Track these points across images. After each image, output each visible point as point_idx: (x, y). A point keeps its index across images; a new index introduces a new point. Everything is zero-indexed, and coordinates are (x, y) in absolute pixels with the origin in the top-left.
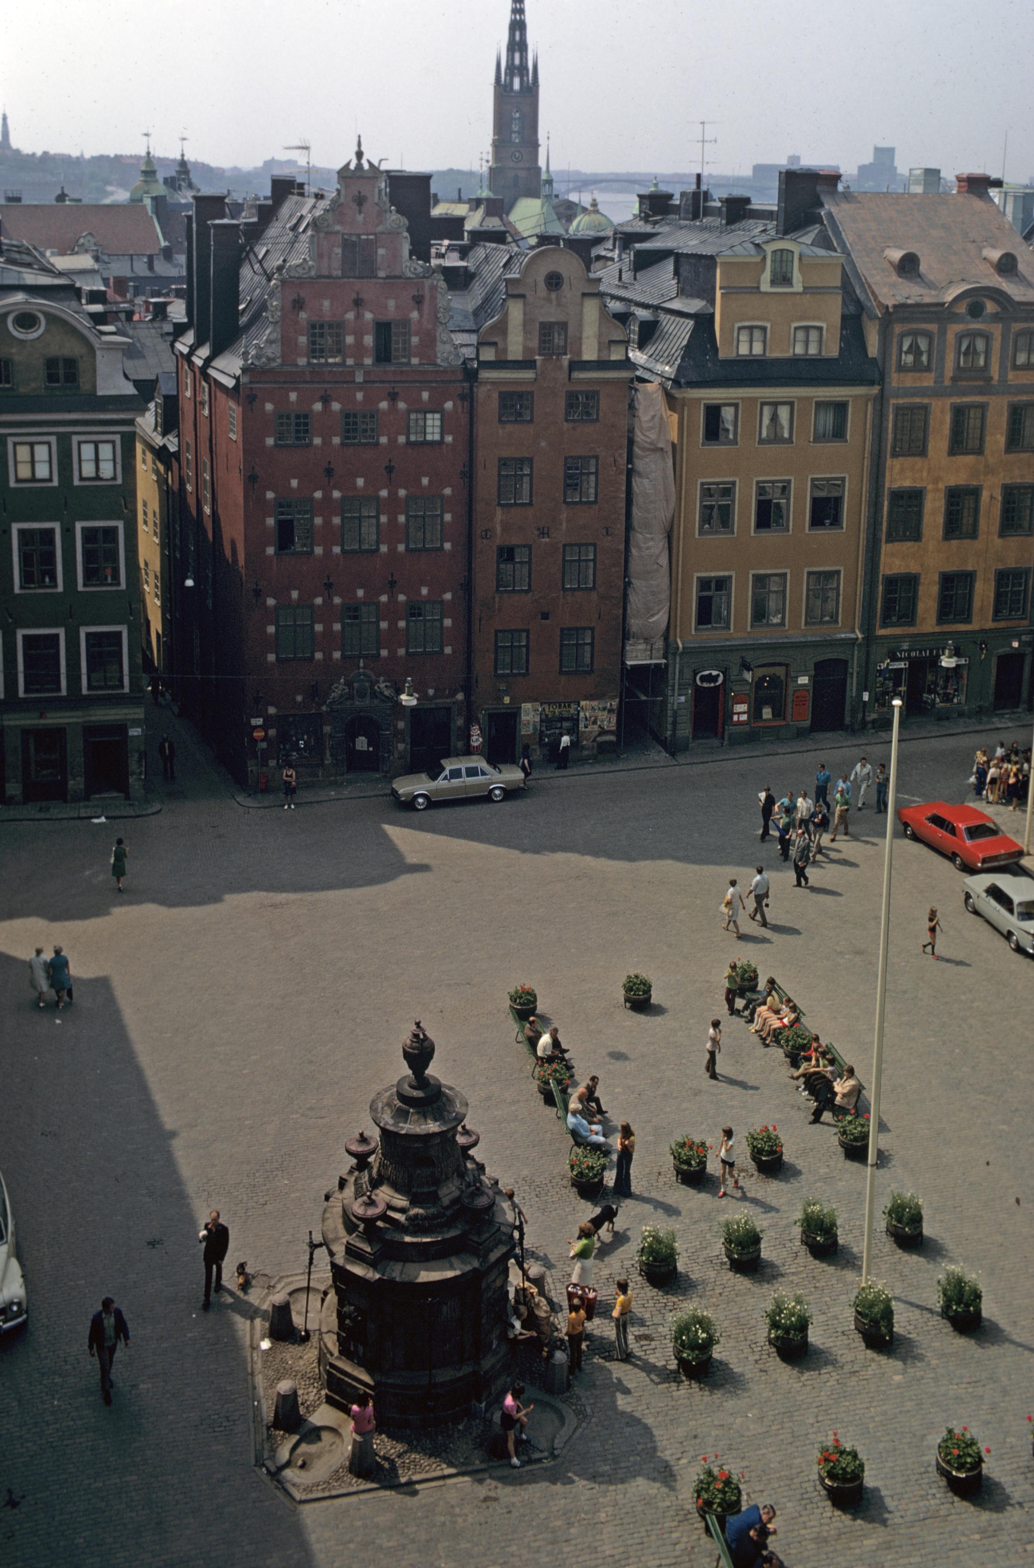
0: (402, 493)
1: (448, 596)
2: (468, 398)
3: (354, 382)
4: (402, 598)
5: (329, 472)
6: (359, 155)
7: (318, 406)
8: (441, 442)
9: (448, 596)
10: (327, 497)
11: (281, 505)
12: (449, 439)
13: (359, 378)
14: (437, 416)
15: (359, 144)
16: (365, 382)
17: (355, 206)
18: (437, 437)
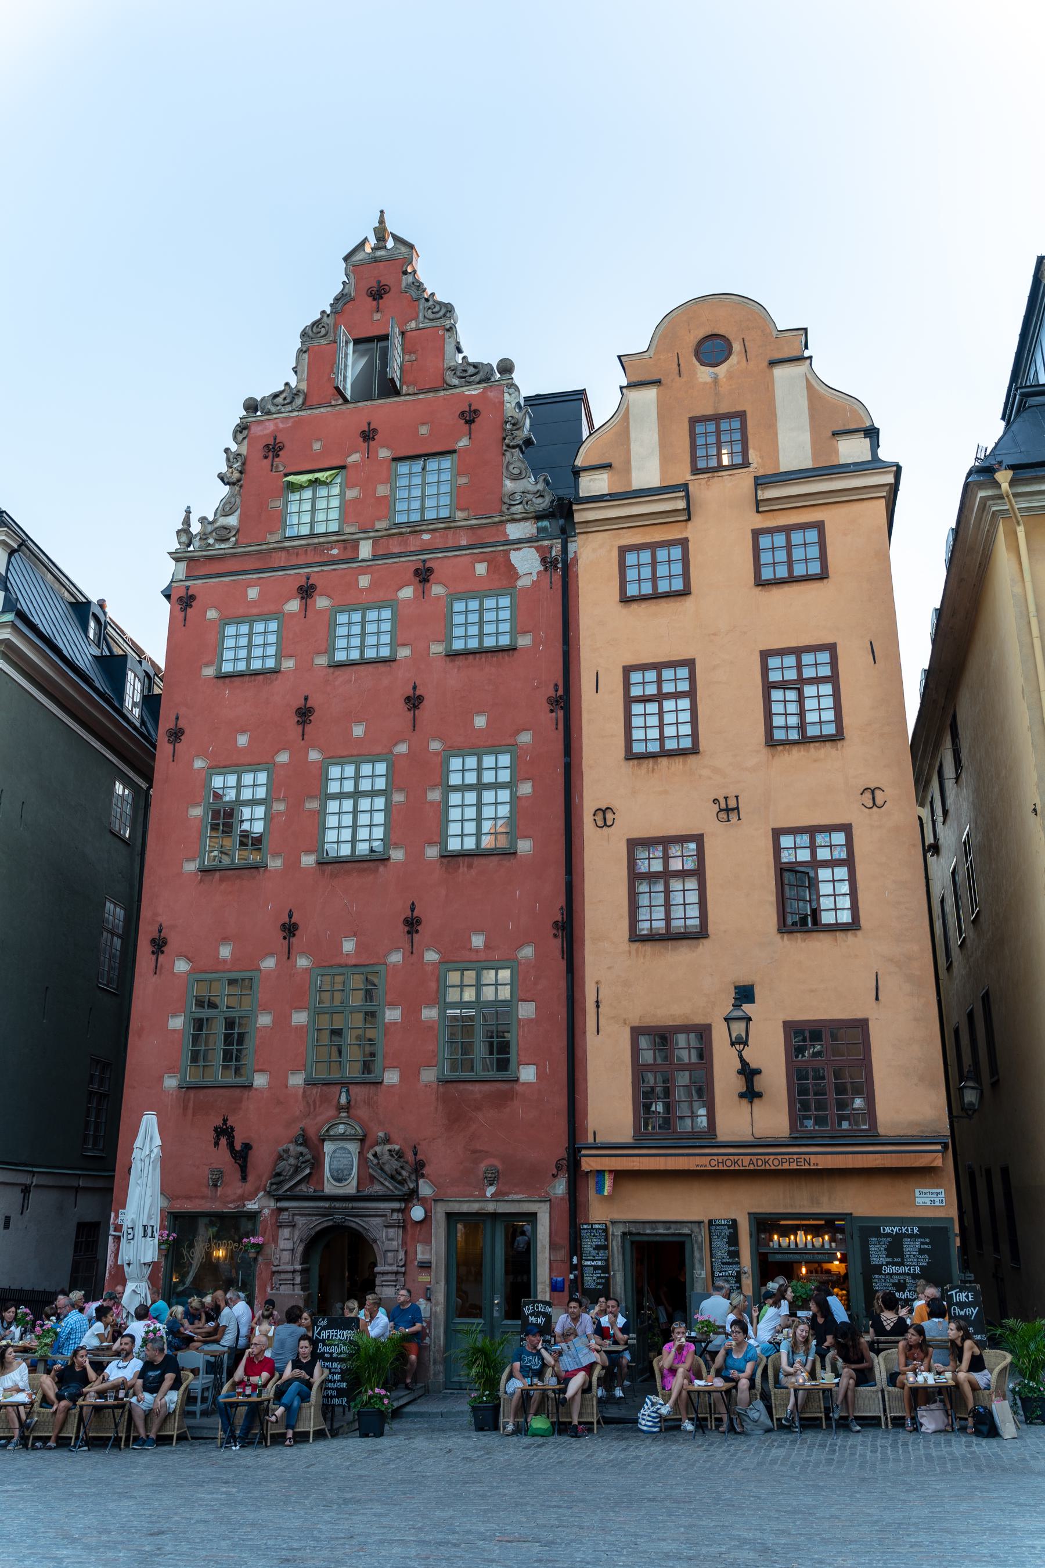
0: (435, 746)
1: (527, 952)
3: (354, 560)
4: (431, 956)
5: (304, 714)
6: (381, 233)
7: (293, 606)
8: (511, 649)
9: (527, 952)
10: (299, 761)
12: (524, 641)
13: (365, 550)
14: (505, 601)
15: (382, 221)
16: (376, 557)
17: (370, 303)
18: (505, 641)
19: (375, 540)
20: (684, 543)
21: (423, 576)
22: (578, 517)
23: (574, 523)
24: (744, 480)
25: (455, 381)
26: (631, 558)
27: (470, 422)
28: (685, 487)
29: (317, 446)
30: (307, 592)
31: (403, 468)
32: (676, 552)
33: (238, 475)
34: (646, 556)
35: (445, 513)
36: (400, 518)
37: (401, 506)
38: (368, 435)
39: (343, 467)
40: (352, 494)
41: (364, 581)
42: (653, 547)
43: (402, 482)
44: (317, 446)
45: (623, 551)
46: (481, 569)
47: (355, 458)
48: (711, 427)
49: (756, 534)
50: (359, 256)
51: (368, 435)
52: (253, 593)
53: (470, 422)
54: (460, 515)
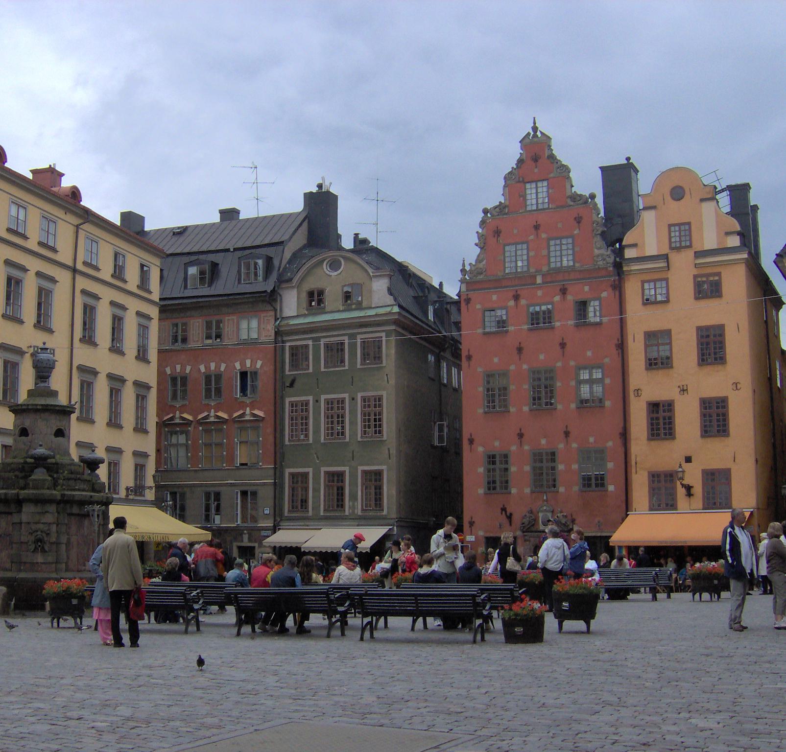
2: (618, 288)
3: (535, 284)
7: (512, 303)
11: (489, 376)
13: (539, 280)
16: (544, 283)
19: (543, 275)
20: (667, 280)
21: (564, 291)
22: (625, 269)
23: (623, 272)
24: (690, 253)
25: (572, 203)
26: (646, 286)
27: (579, 222)
28: (666, 257)
29: (515, 231)
30: (516, 298)
31: (552, 243)
32: (664, 284)
33: (483, 243)
34: (652, 285)
35: (571, 263)
36: (553, 265)
37: (552, 260)
38: (537, 227)
39: (527, 242)
40: (532, 254)
41: (540, 293)
42: (655, 281)
43: (552, 248)
44: (515, 231)
45: (643, 282)
46: (586, 288)
47: (532, 237)
48: (677, 228)
49: (695, 277)
50: (524, 142)
51: (537, 227)
52: (494, 297)
53: (579, 222)
54: (577, 265)
